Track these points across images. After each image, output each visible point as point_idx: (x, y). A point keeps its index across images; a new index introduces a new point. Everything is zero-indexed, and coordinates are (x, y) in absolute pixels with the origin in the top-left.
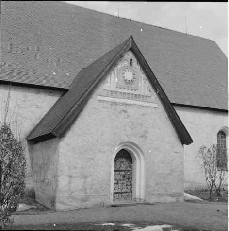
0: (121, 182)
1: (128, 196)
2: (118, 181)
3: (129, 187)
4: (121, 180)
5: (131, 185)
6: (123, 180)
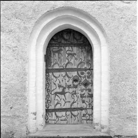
0: (71, 90)
1: (84, 115)
2: (64, 88)
3: (87, 99)
4: (69, 87)
5: (91, 96)
6: (76, 87)
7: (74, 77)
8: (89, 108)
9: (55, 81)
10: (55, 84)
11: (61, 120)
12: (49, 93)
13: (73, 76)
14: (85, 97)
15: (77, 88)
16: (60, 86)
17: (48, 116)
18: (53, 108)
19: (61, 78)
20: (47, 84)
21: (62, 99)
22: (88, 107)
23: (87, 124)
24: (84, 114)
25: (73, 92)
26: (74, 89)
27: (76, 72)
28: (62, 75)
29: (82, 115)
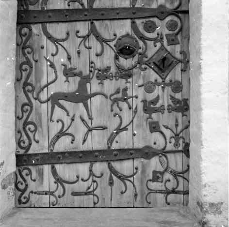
0: (110, 86)
1: (157, 176)
2: (86, 80)
3: (165, 119)
4: (103, 74)
5: (183, 107)
6: (126, 74)
7: (120, 39)
8: (174, 149)
9: (53, 55)
11: (74, 194)
12: (30, 95)
13: (115, 35)
14: (160, 110)
15: (130, 80)
16: (69, 73)
17: (28, 178)
18: (46, 151)
19: (71, 46)
20: (23, 63)
21: (78, 120)
22: (170, 147)
23: (168, 207)
24: (155, 172)
25: (118, 92)
26: (122, 83)
27: (128, 22)
28: (78, 32)
29: (151, 177)
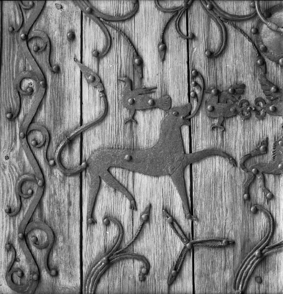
10: (97, 81)
